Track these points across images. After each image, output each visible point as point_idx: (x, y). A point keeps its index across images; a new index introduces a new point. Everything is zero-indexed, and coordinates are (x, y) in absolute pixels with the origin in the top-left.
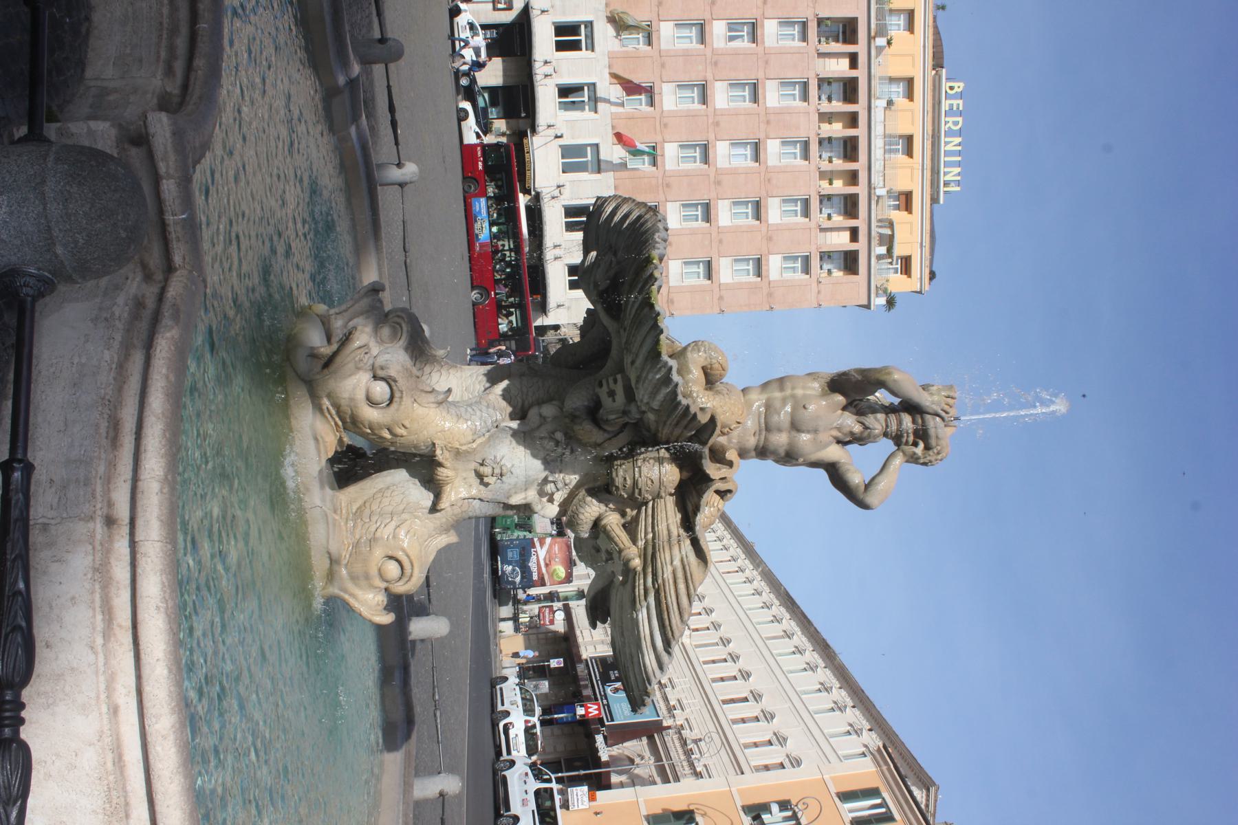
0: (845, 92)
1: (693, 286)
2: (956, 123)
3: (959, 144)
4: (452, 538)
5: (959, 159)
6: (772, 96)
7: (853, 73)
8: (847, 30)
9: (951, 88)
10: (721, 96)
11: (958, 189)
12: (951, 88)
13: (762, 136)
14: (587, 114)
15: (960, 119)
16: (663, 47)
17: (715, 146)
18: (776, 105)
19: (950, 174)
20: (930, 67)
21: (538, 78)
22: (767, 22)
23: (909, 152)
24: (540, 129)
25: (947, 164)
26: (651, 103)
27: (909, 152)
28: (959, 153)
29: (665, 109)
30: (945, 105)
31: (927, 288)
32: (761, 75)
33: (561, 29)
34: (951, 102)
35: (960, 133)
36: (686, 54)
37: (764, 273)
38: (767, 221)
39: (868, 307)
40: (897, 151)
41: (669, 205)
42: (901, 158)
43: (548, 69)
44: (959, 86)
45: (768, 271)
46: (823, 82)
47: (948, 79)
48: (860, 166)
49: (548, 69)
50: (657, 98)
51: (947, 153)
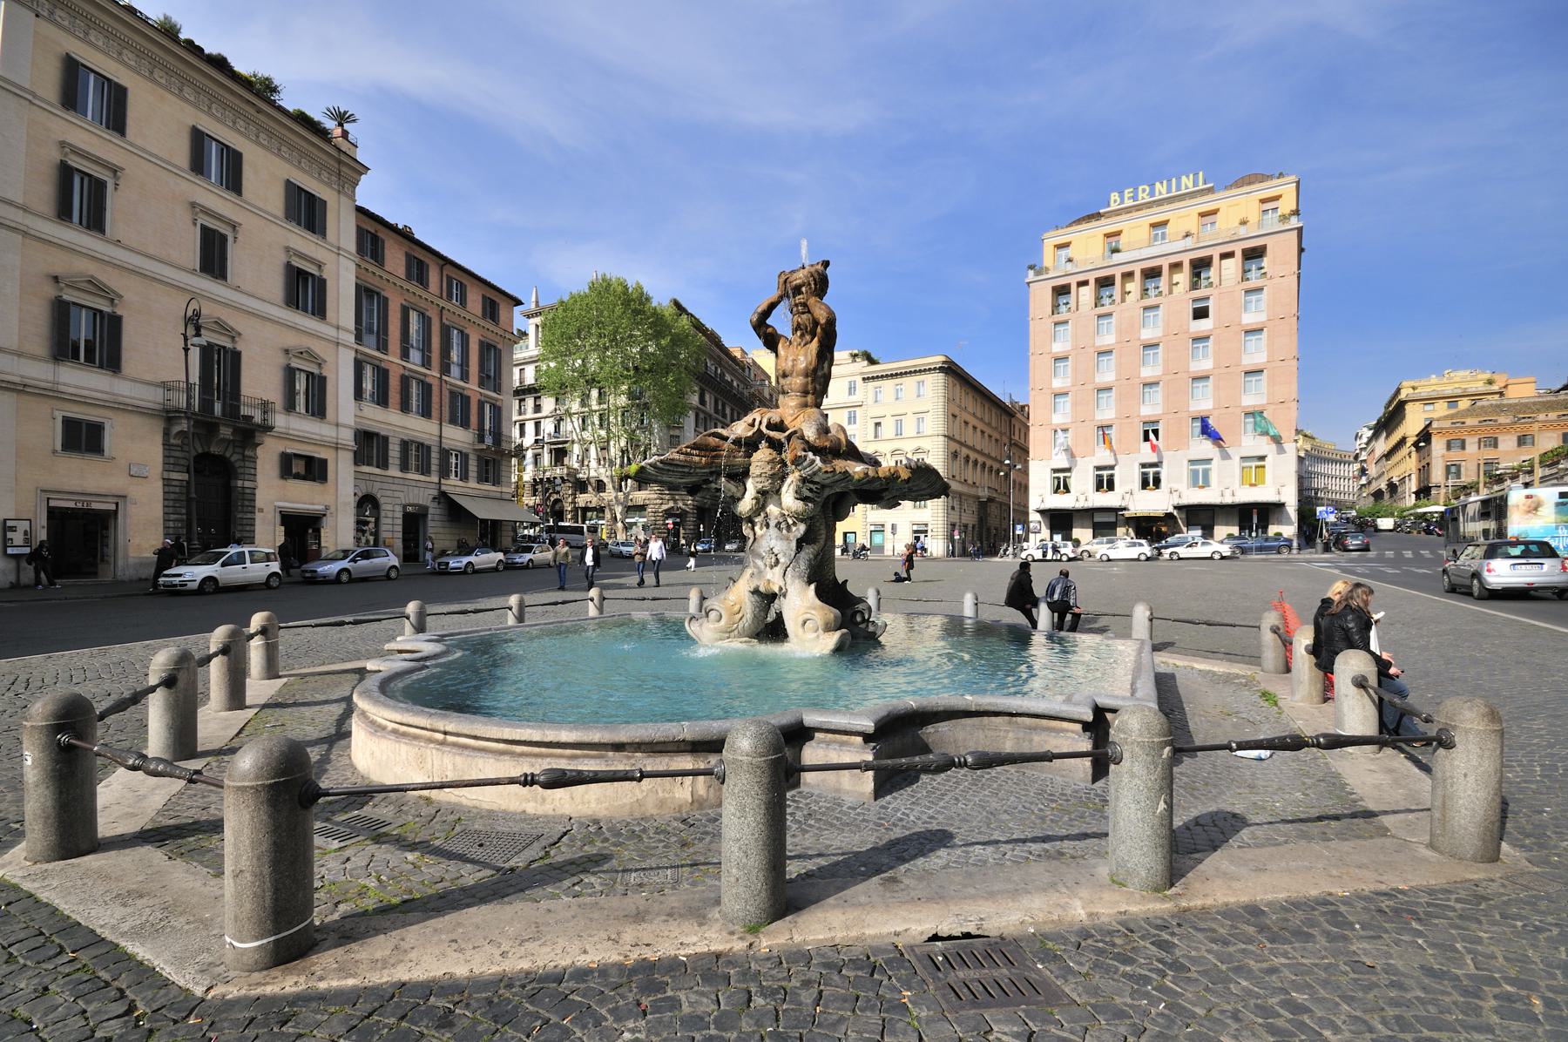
0: (1107, 286)
1: (1268, 385)
2: (1144, 191)
3: (1162, 183)
4: (813, 586)
5: (1174, 180)
6: (1108, 340)
7: (1092, 282)
8: (1061, 291)
9: (1115, 201)
10: (1107, 376)
11: (1201, 173)
12: (1115, 201)
13: (1138, 343)
14: (1116, 472)
15: (1140, 188)
16: (1069, 421)
17: (1145, 378)
18: (1114, 336)
19: (1187, 183)
20: (1098, 222)
21: (1089, 505)
22: (1054, 351)
23: (1164, 223)
24: (1123, 505)
25: (1179, 188)
26: (1110, 426)
27: (1164, 223)
28: (1169, 181)
29: (1114, 416)
30: (1128, 203)
31: (1294, 177)
32: (1092, 350)
33: (1056, 491)
34: (1126, 198)
35: (1152, 186)
36: (1075, 404)
37: (1259, 326)
38: (1211, 330)
39: (1300, 230)
40: (1163, 234)
41: (1191, 409)
42: (1169, 229)
43: (1082, 499)
44: (1114, 196)
45: (1257, 323)
46: (1098, 302)
47: (1109, 206)
48: (1165, 263)
49: (1082, 499)
50: (1105, 423)
51: (1169, 191)
